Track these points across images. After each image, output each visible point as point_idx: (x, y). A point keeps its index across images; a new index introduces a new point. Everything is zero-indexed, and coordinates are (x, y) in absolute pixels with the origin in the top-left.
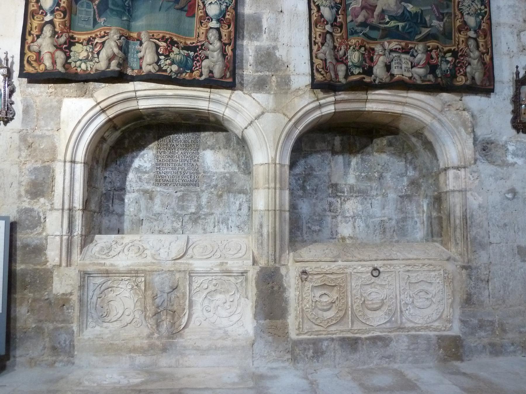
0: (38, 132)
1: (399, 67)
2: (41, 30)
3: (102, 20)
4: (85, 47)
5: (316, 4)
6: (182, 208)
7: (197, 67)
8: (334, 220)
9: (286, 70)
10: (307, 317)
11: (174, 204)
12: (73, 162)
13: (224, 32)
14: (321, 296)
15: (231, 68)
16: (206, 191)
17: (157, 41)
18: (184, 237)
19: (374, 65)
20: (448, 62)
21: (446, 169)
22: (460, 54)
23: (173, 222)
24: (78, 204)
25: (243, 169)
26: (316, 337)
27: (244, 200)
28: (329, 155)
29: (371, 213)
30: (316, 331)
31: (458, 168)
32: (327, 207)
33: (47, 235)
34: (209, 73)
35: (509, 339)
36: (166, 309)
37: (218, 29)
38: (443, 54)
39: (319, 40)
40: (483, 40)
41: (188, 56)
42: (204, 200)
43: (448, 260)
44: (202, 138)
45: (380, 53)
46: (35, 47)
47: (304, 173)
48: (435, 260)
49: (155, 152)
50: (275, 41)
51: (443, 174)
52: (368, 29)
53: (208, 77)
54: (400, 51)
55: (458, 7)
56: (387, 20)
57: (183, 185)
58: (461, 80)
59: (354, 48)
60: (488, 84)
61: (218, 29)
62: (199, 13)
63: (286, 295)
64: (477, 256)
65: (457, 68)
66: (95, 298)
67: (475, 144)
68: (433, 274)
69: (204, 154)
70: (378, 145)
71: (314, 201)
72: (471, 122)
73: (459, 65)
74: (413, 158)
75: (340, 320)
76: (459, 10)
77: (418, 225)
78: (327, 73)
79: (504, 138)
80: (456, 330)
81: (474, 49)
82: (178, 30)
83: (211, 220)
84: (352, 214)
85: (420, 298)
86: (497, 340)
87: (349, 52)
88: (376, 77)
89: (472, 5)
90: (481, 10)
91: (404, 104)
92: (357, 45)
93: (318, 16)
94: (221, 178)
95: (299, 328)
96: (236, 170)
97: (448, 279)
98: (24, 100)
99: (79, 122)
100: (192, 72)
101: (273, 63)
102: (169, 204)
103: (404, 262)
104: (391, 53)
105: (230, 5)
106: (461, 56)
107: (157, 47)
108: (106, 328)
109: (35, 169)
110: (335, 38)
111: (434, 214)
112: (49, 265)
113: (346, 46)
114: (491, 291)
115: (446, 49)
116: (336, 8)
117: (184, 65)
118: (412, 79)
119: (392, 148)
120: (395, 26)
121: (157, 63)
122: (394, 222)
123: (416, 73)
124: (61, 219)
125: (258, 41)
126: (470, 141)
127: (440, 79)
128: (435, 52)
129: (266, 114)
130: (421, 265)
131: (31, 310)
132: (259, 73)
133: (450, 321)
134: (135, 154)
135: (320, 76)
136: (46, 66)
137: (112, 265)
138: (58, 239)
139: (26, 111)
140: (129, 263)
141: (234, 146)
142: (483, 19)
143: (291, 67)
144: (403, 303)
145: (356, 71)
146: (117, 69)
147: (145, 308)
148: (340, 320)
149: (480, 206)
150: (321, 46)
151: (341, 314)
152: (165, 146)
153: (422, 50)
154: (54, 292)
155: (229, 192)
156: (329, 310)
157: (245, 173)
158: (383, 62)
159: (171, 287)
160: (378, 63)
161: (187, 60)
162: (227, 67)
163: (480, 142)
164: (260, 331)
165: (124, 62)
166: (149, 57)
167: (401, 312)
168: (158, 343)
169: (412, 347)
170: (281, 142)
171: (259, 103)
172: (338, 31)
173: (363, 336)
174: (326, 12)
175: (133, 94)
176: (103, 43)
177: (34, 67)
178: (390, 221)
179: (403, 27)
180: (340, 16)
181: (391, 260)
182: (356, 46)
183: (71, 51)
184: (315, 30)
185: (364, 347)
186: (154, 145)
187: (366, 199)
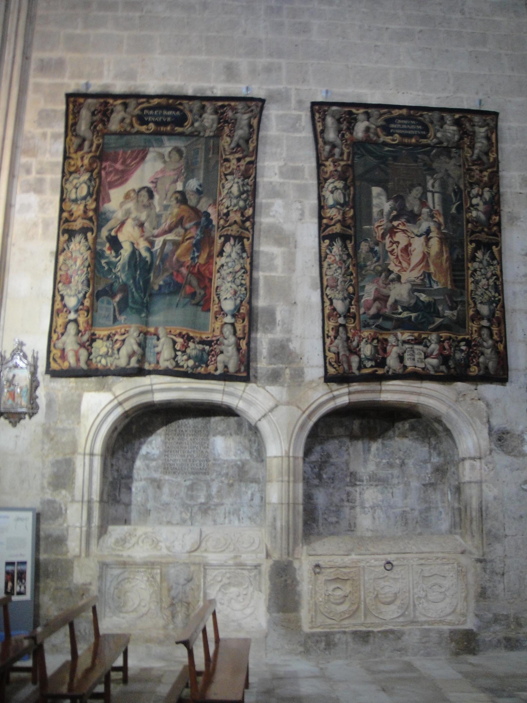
0: (60, 426)
2: (66, 328)
3: (122, 318)
4: (105, 343)
5: (329, 297)
6: (192, 497)
7: (212, 361)
8: (352, 511)
10: (320, 610)
11: (182, 494)
12: (92, 454)
13: (239, 326)
14: (334, 590)
15: (245, 363)
16: (216, 480)
17: (174, 337)
18: (196, 529)
20: (462, 351)
21: (463, 459)
22: (473, 343)
23: (181, 513)
24: (96, 497)
25: (256, 457)
26: (328, 630)
27: (257, 490)
28: (346, 440)
29: (392, 503)
30: (330, 625)
31: (474, 459)
32: (344, 497)
33: (68, 526)
35: (524, 633)
36: (181, 601)
37: (233, 325)
38: (456, 343)
39: (332, 333)
40: (497, 329)
41: (204, 350)
42: (214, 490)
43: (463, 553)
44: (212, 423)
45: (394, 344)
46: (60, 345)
47: (320, 460)
48: (449, 553)
49: (163, 437)
51: (461, 463)
52: (381, 320)
53: (222, 372)
54: (413, 342)
55: (471, 296)
56: (400, 310)
57: (193, 473)
58: (474, 370)
59: (366, 341)
60: (502, 373)
61: (233, 325)
62: (214, 308)
63: (299, 588)
64: (492, 548)
65: (471, 358)
66: (112, 589)
67: (490, 434)
68: (447, 567)
69: (214, 441)
70: (399, 429)
71: (331, 490)
72: (486, 412)
73: (472, 355)
74: (437, 443)
75: (353, 614)
76: (473, 298)
77: (443, 516)
78: (339, 366)
79: (521, 428)
80: (470, 624)
81: (488, 338)
82: (194, 325)
83: (221, 510)
84: (371, 504)
85: (433, 592)
86: (512, 635)
89: (485, 293)
90: (494, 297)
91: (419, 394)
94: (232, 467)
95: (312, 622)
96: (248, 458)
97: (461, 572)
98: (48, 394)
99: (98, 415)
100: (207, 366)
102: (178, 494)
103: (418, 555)
105: (244, 299)
106: (475, 345)
107: (175, 343)
108: (123, 618)
109: (57, 462)
110: (349, 329)
111: (456, 505)
112: (70, 555)
113: (360, 338)
114: (506, 584)
115: (460, 337)
116: (350, 299)
117: (201, 360)
119: (415, 433)
120: (407, 317)
121: (174, 358)
122: (416, 513)
123: (429, 363)
124: (80, 510)
125: (271, 333)
126: (486, 431)
127: (453, 370)
128: (448, 343)
129: (280, 407)
130: (434, 559)
131: (54, 598)
132: (273, 366)
133: (464, 615)
134: (142, 440)
135: (334, 370)
136: (70, 363)
137: (129, 556)
138: (78, 530)
139: (50, 404)
140: (146, 554)
141: (245, 432)
142: (496, 307)
143: (305, 359)
144: (416, 596)
146: (136, 365)
147: (161, 599)
148: (353, 614)
149: (495, 498)
150: (333, 340)
151: (354, 607)
152: (174, 432)
153: (435, 340)
154: (75, 581)
155: (241, 481)
156: (341, 603)
157: (257, 461)
158: (396, 352)
159: (185, 580)
161: (202, 354)
162: (241, 362)
163: (495, 432)
164: (273, 623)
165: (142, 359)
166: (166, 353)
167: (414, 605)
168: (173, 633)
169: (424, 640)
170: (294, 435)
171: (272, 396)
173: (376, 630)
174: (340, 306)
175: (149, 388)
176: (124, 341)
177: (59, 364)
178: (413, 512)
179: (416, 318)
180: (353, 307)
181: (404, 553)
182: (368, 339)
183: (92, 348)
184: (328, 323)
185: (376, 640)
186: (162, 431)
187: (386, 488)
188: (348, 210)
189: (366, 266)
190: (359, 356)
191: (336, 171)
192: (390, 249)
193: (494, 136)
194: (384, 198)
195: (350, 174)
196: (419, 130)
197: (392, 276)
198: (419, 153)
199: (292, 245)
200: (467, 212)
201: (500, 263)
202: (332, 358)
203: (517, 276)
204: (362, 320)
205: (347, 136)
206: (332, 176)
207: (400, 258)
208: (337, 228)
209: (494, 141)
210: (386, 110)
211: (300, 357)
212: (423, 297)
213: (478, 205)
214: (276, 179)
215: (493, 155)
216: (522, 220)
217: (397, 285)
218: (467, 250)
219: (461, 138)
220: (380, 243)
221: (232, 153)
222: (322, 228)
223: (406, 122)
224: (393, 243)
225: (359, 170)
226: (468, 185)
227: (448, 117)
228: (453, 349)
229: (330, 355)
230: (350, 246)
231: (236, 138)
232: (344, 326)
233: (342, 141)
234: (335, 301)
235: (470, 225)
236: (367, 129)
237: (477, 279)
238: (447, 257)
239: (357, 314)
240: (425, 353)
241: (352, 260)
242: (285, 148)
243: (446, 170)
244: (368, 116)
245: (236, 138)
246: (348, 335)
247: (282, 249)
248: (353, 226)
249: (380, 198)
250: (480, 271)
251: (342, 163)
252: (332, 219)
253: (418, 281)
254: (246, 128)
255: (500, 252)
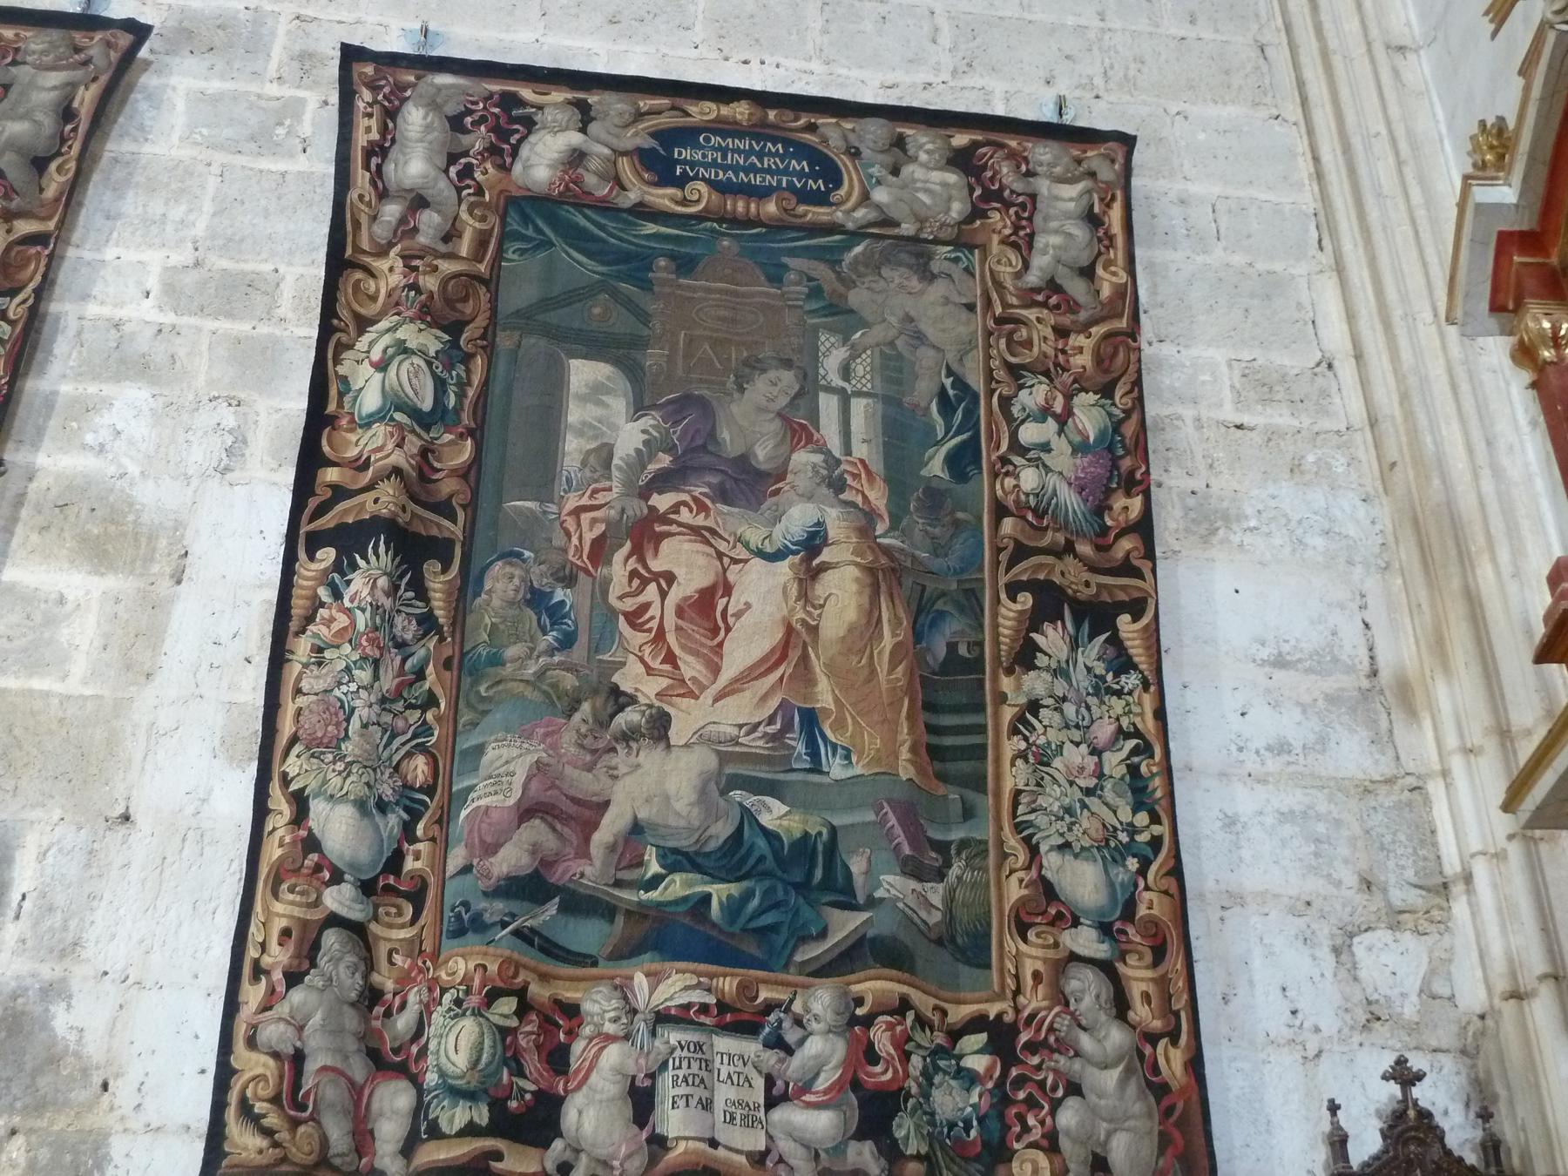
1: (693, 1102)
5: (294, 787)
9: (91, 1106)
19: (571, 1086)
20: (970, 1079)
22: (1024, 1037)
38: (940, 1039)
39: (278, 957)
40: (1149, 974)
45: (609, 1028)
50: (63, 954)
52: (552, 908)
55: (1014, 816)
56: (654, 868)
59: (458, 1002)
73: (1021, 1095)
76: (1018, 827)
78: (295, 1124)
81: (1103, 1017)
87: (437, 1017)
88: (577, 1151)
89: (1084, 806)
90: (1132, 830)
92: (477, 982)
93: (294, 842)
101: (29, 1066)
104: (659, 1030)
106: (1032, 1047)
110: (382, 950)
113: (430, 990)
115: (959, 1013)
116: (407, 809)
118: (769, 1164)
120: (685, 899)
128: (890, 1027)
135: (260, 1142)
142: (1143, 871)
143: (123, 1092)
145: (454, 1116)
150: (281, 988)
153: (830, 1017)
158: (618, 1071)
160: (594, 1078)
172: (400, 914)
179: (734, 908)
180: (420, 846)
182: (468, 992)
184: (267, 910)
188: (451, 443)
189: (496, 661)
190: (416, 1081)
191: (414, 287)
192: (630, 605)
193: (1115, 215)
194: (619, 405)
195: (477, 307)
196: (801, 175)
197: (629, 717)
198: (792, 253)
199: (161, 567)
200: (995, 475)
201: (1155, 683)
202: (262, 1077)
203: (1240, 749)
204: (448, 901)
205: (487, 173)
206: (393, 305)
207: (671, 638)
208: (385, 500)
209: (1117, 228)
210: (664, 102)
211: (97, 1080)
212: (774, 814)
213: (1046, 447)
214: (146, 312)
215: (1114, 274)
216: (1252, 524)
217: (649, 758)
218: (995, 626)
219: (977, 213)
220: (582, 575)
222: (313, 503)
223: (744, 144)
224: (640, 579)
225: (519, 294)
226: (1000, 374)
227: (924, 140)
228: (916, 1062)
229: (253, 1065)
230: (438, 582)
232: (357, 931)
233: (459, 190)
234: (317, 807)
235: (1008, 525)
236: (577, 158)
237: (1041, 741)
238: (897, 647)
239: (432, 880)
240: (770, 1081)
241: (442, 639)
242: (208, 207)
243: (909, 319)
244: (585, 117)
246: (376, 978)
247: (113, 582)
248: (464, 507)
249: (600, 403)
250: (1058, 709)
251: (447, 267)
252: (366, 465)
253: (756, 744)
254: (48, 123)
255: (1153, 636)
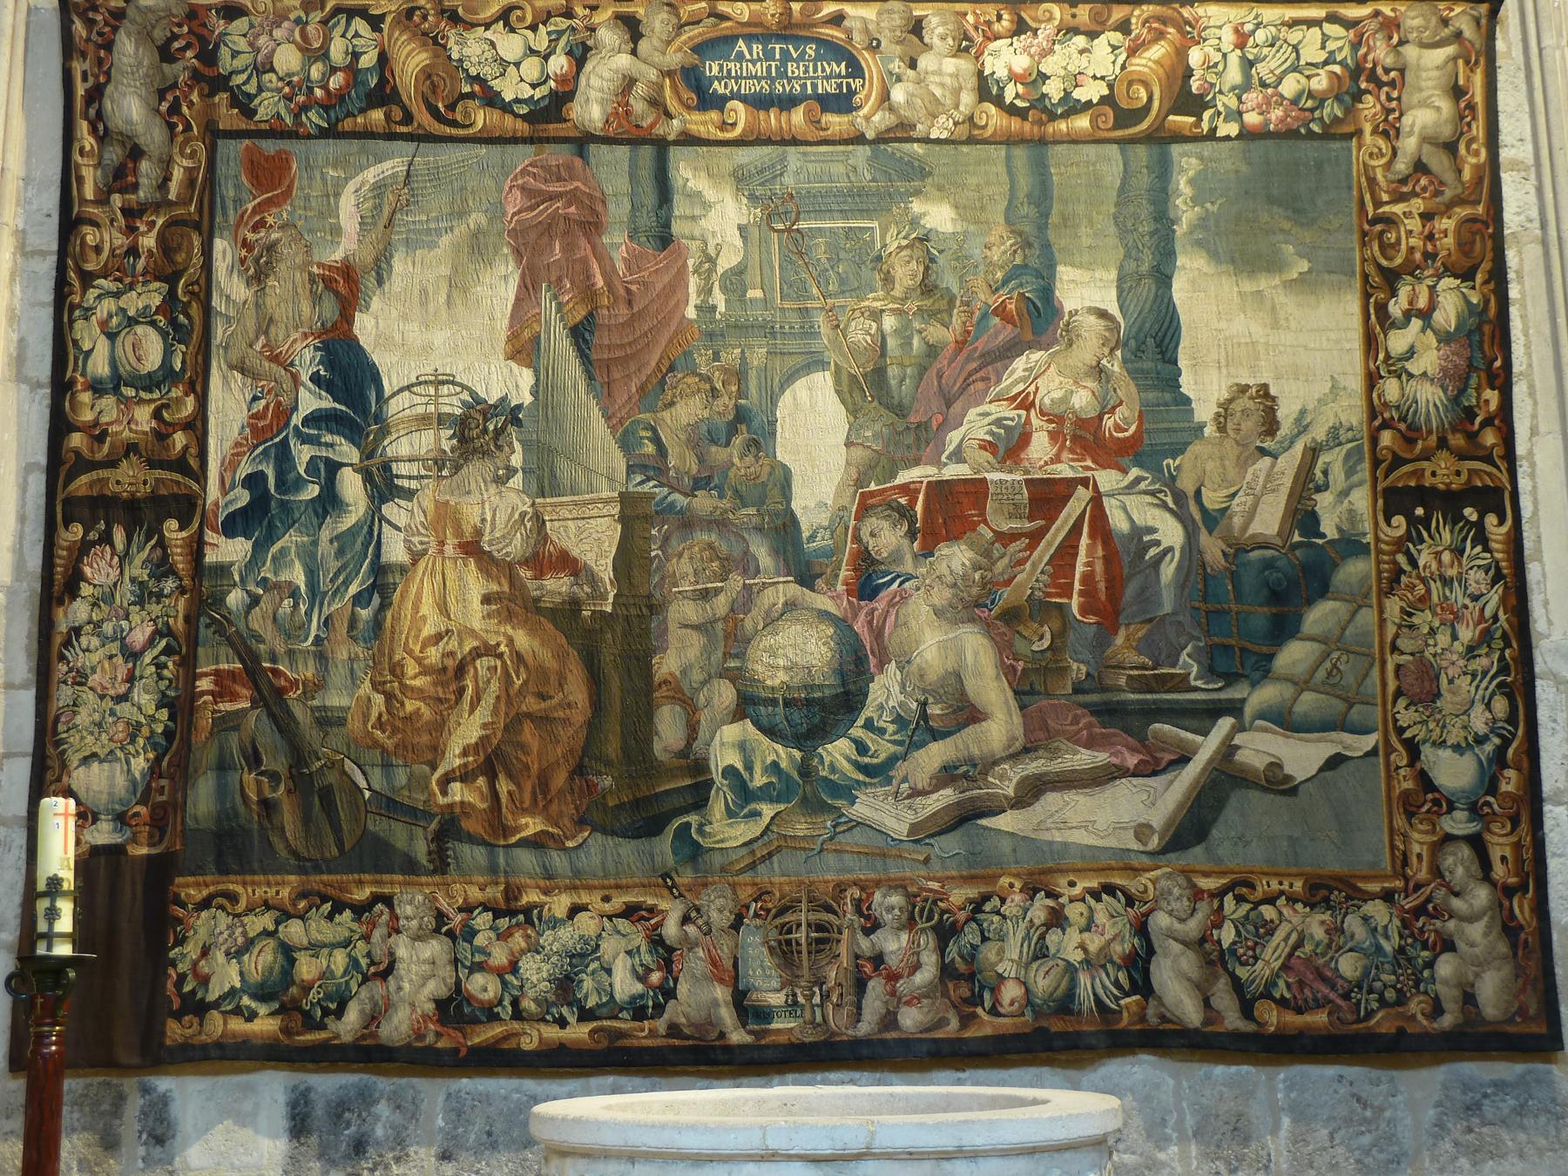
34: (1465, 1003)
221: (1400, 198)
231: (1409, 144)
245: (1409, 144)
254: (1446, 105)
